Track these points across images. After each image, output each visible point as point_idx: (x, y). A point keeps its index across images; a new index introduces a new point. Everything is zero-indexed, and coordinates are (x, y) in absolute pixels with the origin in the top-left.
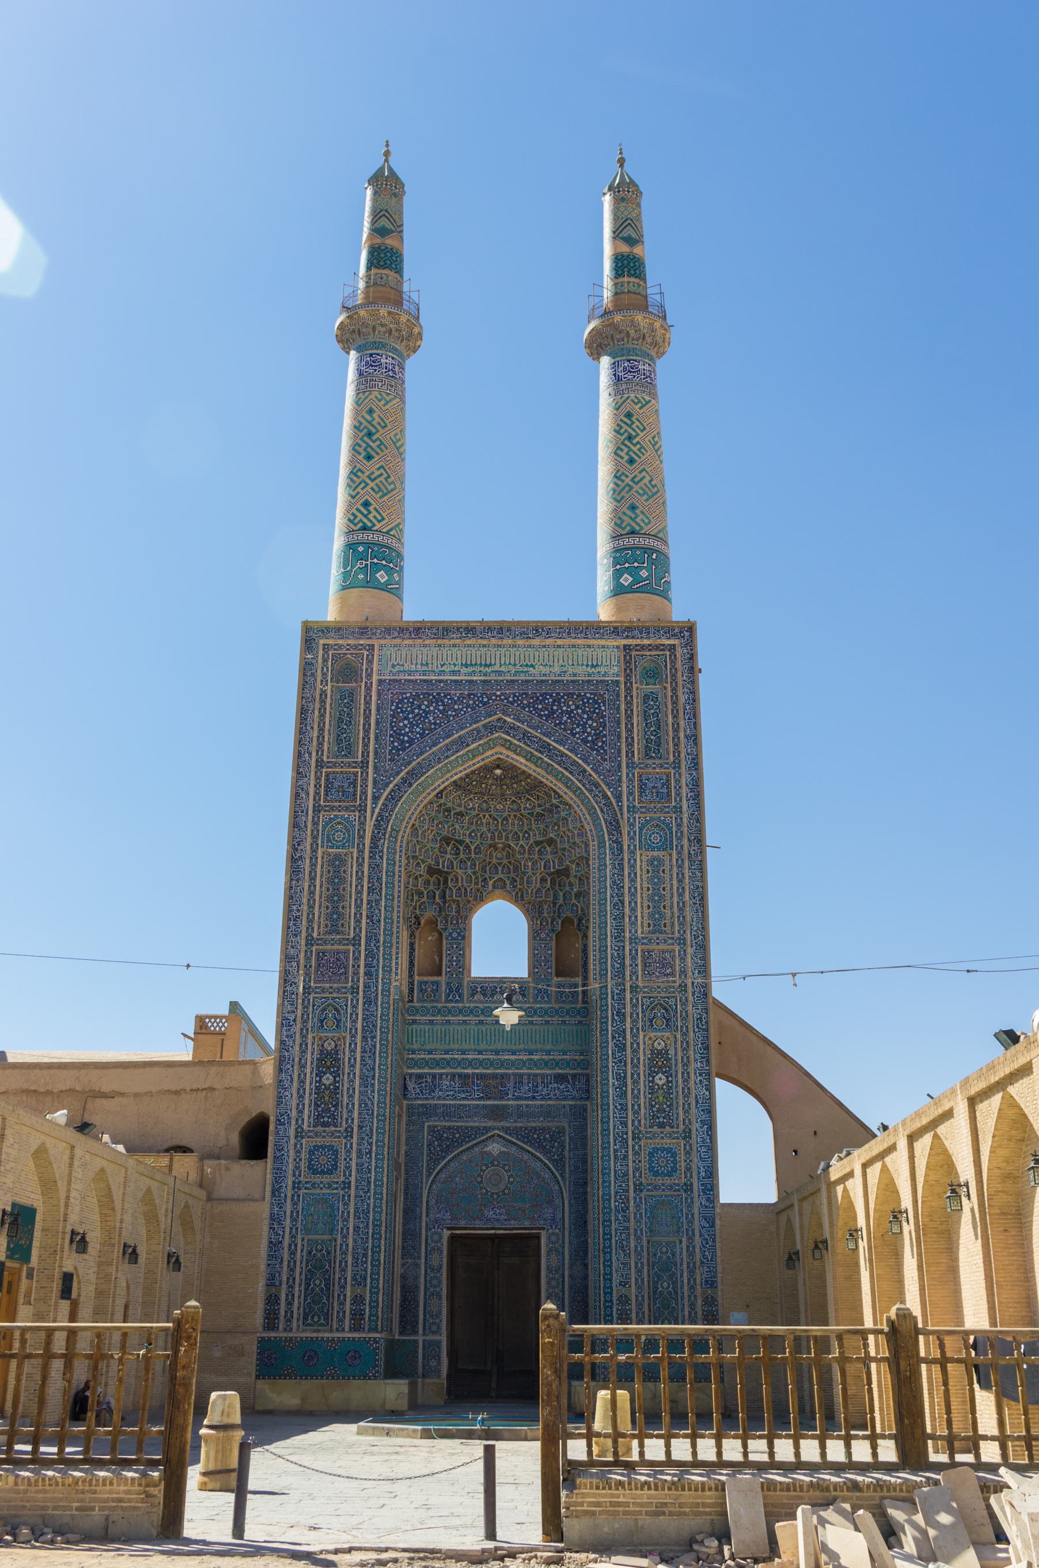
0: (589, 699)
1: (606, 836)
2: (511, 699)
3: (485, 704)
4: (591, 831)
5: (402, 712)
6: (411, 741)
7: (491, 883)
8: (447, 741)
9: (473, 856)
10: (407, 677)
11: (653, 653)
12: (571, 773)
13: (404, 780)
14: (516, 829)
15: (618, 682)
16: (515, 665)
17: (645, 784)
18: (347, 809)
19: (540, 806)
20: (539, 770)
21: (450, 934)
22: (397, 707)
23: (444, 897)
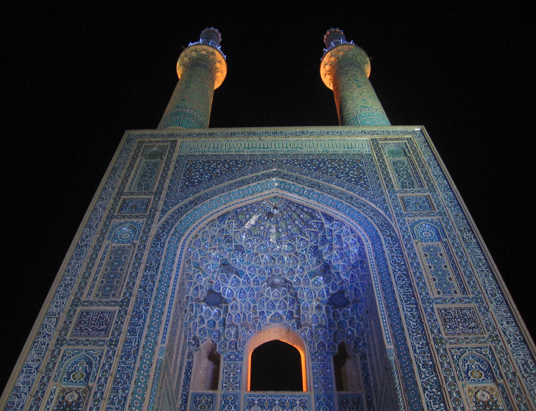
0: (348, 162)
1: (380, 233)
2: (285, 162)
3: (263, 164)
4: (364, 235)
5: (195, 168)
6: (200, 182)
7: (268, 318)
8: (231, 182)
9: (252, 285)
10: (201, 153)
11: (394, 142)
12: (340, 198)
13: (191, 202)
14: (291, 266)
15: (370, 155)
16: (287, 147)
17: (408, 202)
18: (137, 217)
19: (311, 241)
20: (311, 201)
21: (229, 356)
22: (191, 166)
23: (224, 325)
